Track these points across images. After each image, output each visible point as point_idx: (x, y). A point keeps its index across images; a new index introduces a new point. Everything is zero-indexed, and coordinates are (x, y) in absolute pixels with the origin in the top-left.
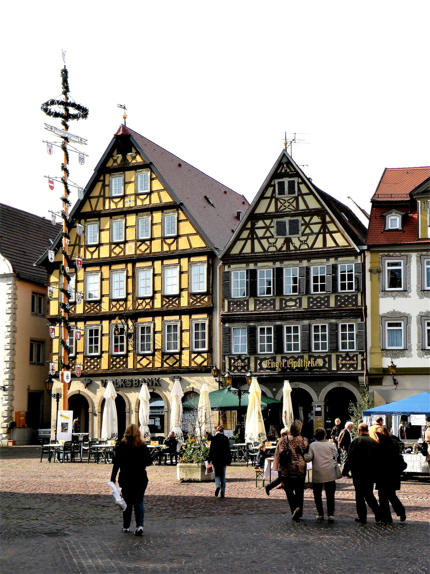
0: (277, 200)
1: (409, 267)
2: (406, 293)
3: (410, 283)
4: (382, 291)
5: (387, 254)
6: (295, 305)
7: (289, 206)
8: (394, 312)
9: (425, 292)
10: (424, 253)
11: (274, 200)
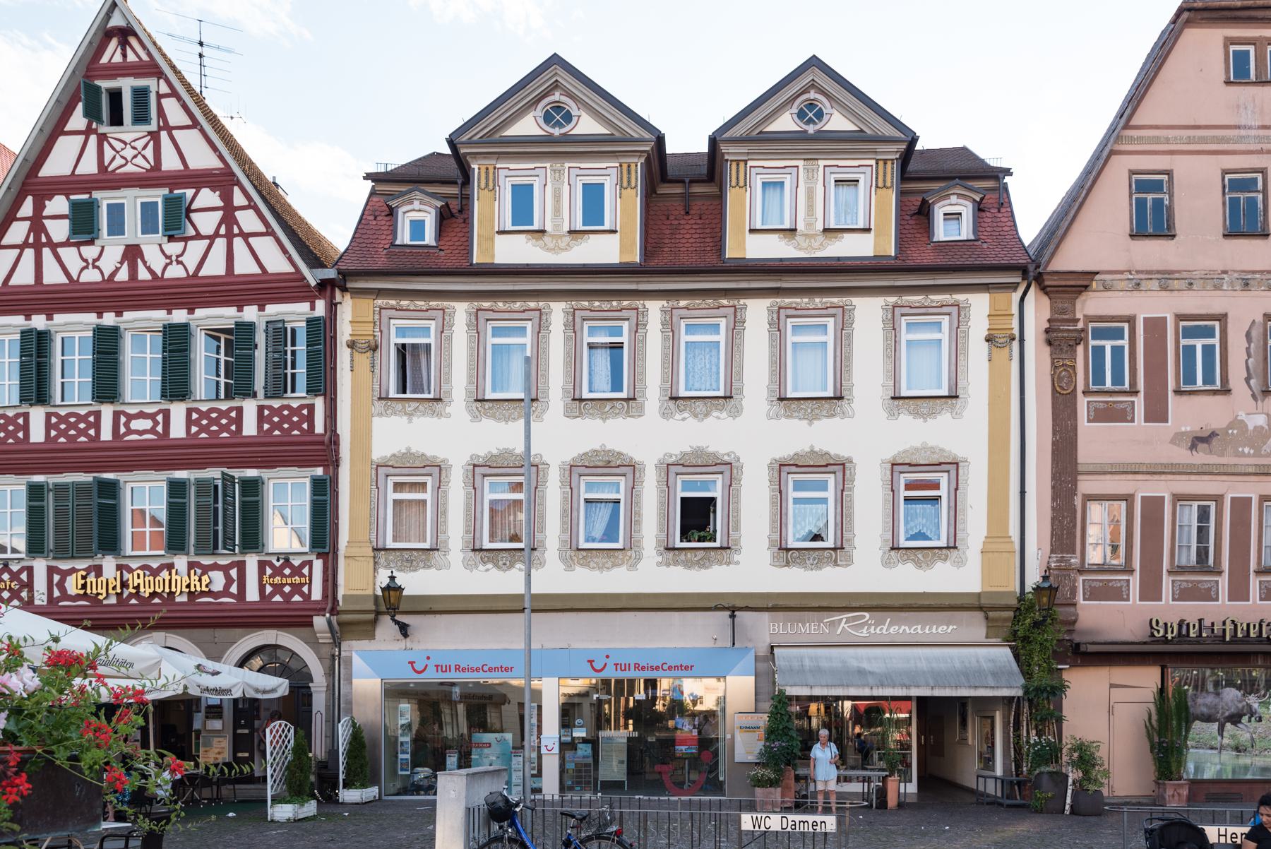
0: (102, 138)
1: (449, 339)
2: (439, 406)
3: (448, 381)
4: (380, 399)
5: (393, 302)
6: (152, 430)
7: (135, 157)
8: (408, 454)
9: (487, 405)
10: (486, 305)
11: (93, 139)
